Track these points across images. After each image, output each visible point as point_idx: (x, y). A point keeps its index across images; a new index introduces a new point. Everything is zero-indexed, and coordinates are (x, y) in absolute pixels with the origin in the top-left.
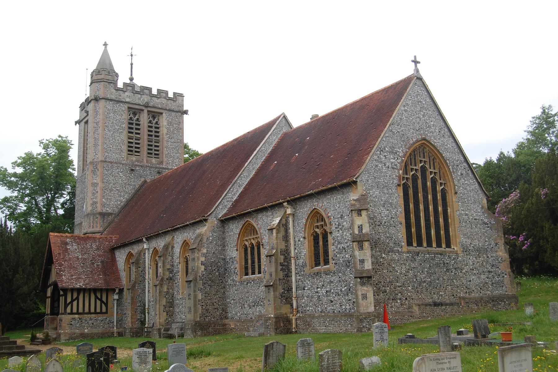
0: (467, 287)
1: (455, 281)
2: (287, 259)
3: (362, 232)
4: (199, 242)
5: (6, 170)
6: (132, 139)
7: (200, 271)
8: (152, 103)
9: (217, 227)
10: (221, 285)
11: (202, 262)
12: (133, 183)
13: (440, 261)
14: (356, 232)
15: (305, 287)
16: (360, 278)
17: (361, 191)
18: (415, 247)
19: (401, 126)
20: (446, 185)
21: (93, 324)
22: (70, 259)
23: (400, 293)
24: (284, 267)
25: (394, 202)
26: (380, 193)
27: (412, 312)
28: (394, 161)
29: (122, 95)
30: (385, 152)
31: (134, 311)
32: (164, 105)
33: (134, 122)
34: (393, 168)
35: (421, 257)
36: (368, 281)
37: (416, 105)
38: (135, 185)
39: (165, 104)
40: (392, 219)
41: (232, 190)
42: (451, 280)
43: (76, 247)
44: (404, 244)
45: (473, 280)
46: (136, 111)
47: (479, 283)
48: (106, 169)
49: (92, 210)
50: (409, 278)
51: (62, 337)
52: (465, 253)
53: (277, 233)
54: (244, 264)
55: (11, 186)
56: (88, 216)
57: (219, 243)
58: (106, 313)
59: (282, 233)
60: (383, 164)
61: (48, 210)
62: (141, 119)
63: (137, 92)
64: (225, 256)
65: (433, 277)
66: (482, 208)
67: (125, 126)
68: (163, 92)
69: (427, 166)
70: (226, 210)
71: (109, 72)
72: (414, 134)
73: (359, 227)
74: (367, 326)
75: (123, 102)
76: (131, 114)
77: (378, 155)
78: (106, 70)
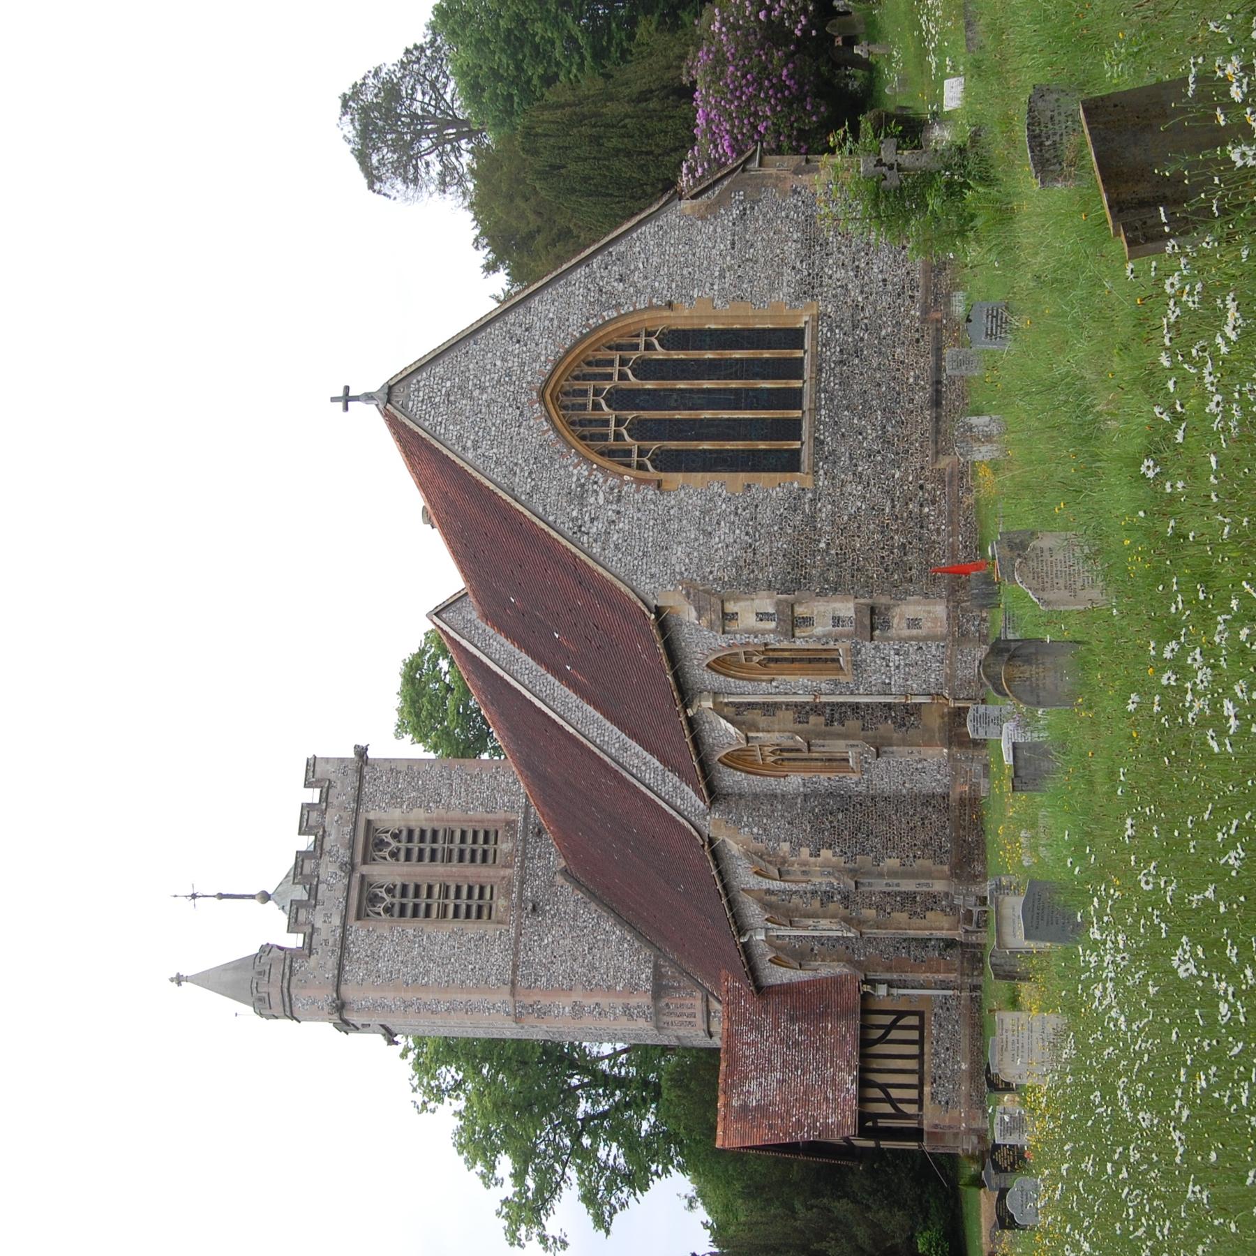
0: (899, 295)
1: (883, 333)
2: (817, 709)
3: (771, 615)
4: (764, 860)
5: (505, 1202)
6: (446, 906)
7: (834, 859)
8: (341, 851)
9: (729, 814)
10: (868, 807)
11: (811, 855)
12: (572, 907)
13: (835, 376)
14: (773, 625)
15: (884, 683)
16: (873, 629)
17: (677, 596)
18: (802, 444)
19: (516, 464)
20: (649, 329)
21: (948, 1049)
22: (784, 1101)
23: (907, 504)
24: (837, 716)
25: (699, 502)
26: (680, 543)
27: (952, 475)
28: (601, 494)
29: (323, 936)
30: (582, 519)
31: (920, 964)
32: (345, 815)
33: (397, 901)
34: (619, 500)
35: (827, 434)
36: (881, 614)
37: (457, 410)
38: (576, 902)
40: (739, 511)
41: (634, 771)
42: (880, 343)
43: (754, 1083)
44: (796, 481)
46: (365, 895)
47: (891, 252)
48: (535, 983)
49: (646, 1018)
50: (877, 475)
51: (978, 1124)
52: (816, 291)
53: (758, 731)
54: (819, 764)
55: (548, 1189)
56: (663, 1028)
57: (766, 808)
58: (921, 1015)
59: (756, 716)
60: (612, 527)
61: (621, 1083)
62: (388, 881)
63: (313, 893)
64: (798, 795)
65: (872, 399)
66: (703, 218)
67: (410, 927)
69: (608, 387)
70: (686, 788)
71: (260, 973)
72: (531, 424)
73: (761, 620)
74: (976, 623)
75: (344, 932)
76: (376, 909)
77: (591, 540)
78: (255, 981)
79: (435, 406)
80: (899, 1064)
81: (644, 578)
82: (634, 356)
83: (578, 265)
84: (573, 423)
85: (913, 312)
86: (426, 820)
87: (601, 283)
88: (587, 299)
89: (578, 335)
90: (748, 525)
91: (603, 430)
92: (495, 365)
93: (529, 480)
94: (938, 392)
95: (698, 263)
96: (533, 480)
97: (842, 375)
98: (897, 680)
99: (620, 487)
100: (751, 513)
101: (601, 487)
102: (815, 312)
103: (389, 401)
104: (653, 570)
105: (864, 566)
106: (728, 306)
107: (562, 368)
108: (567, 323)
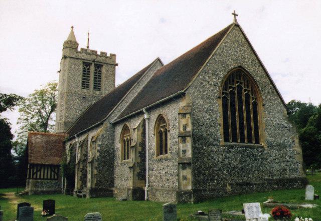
2: (144, 149)
14: (182, 129)
33: (87, 70)
44: (222, 140)
53: (138, 131)
58: (57, 179)
67: (81, 72)
79: (235, 37)
80: (46, 175)
82: (250, 94)
98: (154, 173)
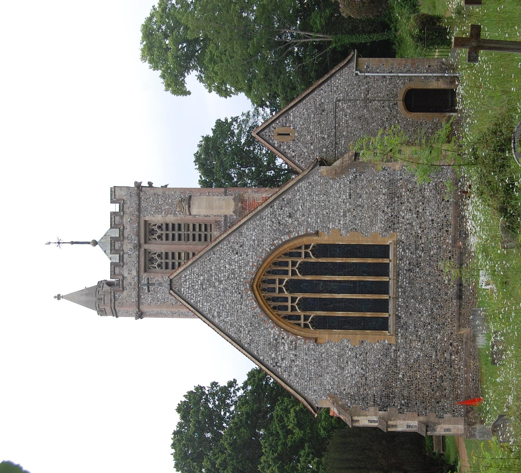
0: (441, 230)
1: (432, 253)
13: (406, 278)
17: (328, 403)
18: (390, 315)
23: (443, 353)
25: (337, 350)
26: (328, 373)
27: (467, 338)
28: (286, 345)
30: (278, 358)
33: (164, 261)
34: (296, 349)
36: (431, 427)
39: (132, 217)
40: (358, 356)
42: (430, 259)
45: (431, 215)
46: (147, 259)
47: (436, 203)
50: (428, 337)
60: (293, 363)
68: (114, 221)
71: (99, 299)
72: (247, 303)
75: (139, 279)
76: (154, 266)
77: (282, 370)
78: (97, 303)
79: (196, 291)
81: (310, 392)
82: (300, 261)
83: (267, 206)
84: (269, 299)
85: (447, 241)
86: (175, 220)
87: (279, 218)
88: (272, 229)
89: (269, 250)
90: (362, 364)
91: (285, 304)
92: (225, 267)
93: (249, 336)
94: (460, 290)
95: (331, 207)
96: (250, 336)
97: (410, 278)
99: (296, 341)
100: (364, 357)
101: (286, 341)
102: (395, 239)
103: (171, 289)
104: (315, 388)
105: (422, 388)
106: (348, 234)
107: (261, 270)
108: (262, 243)
